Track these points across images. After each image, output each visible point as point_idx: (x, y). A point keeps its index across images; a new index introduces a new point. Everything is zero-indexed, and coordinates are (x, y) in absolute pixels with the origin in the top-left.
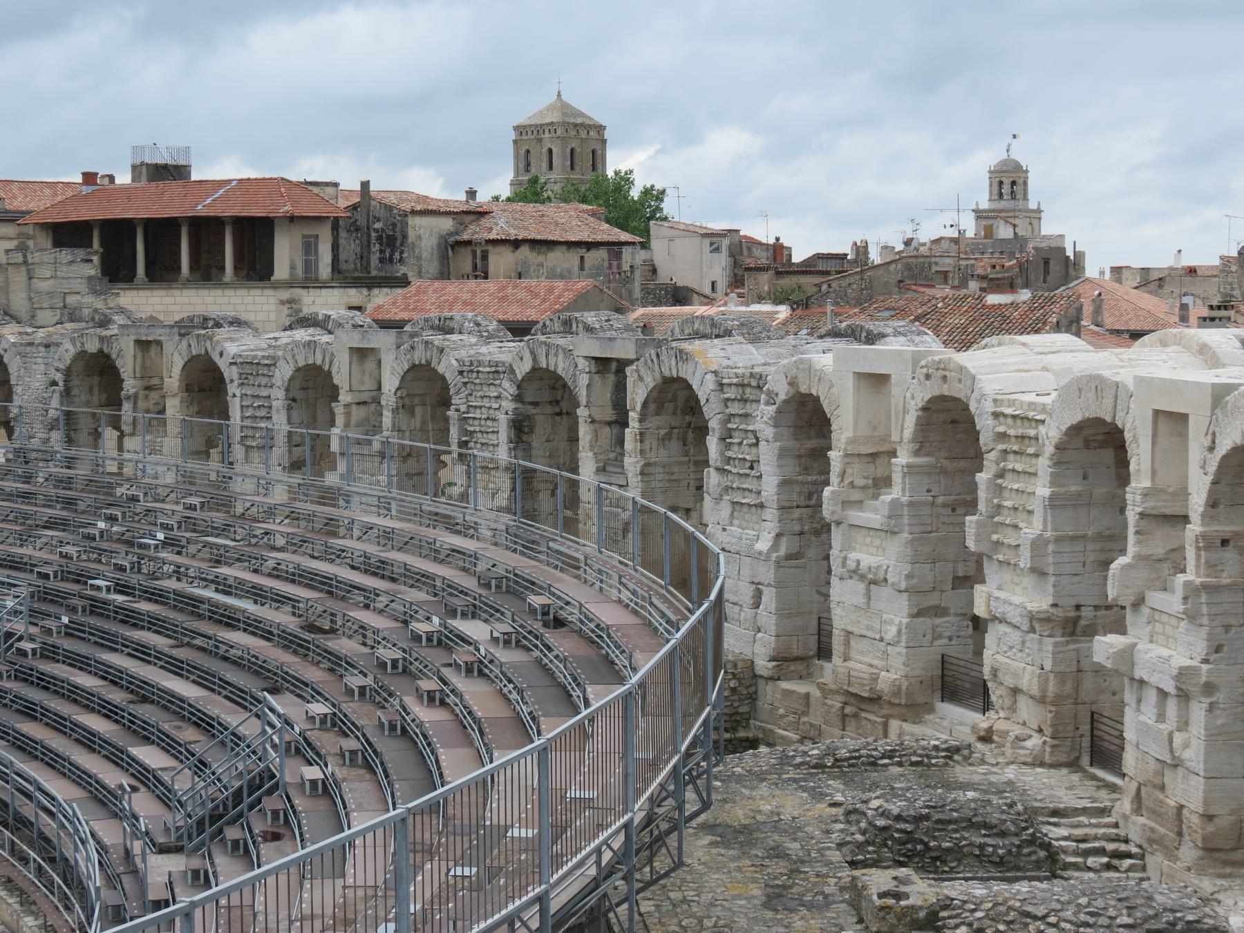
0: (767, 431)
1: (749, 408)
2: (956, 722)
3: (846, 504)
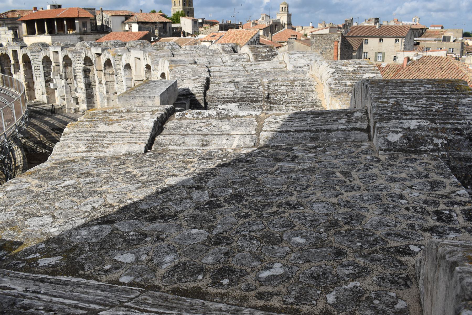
0: (123, 73)
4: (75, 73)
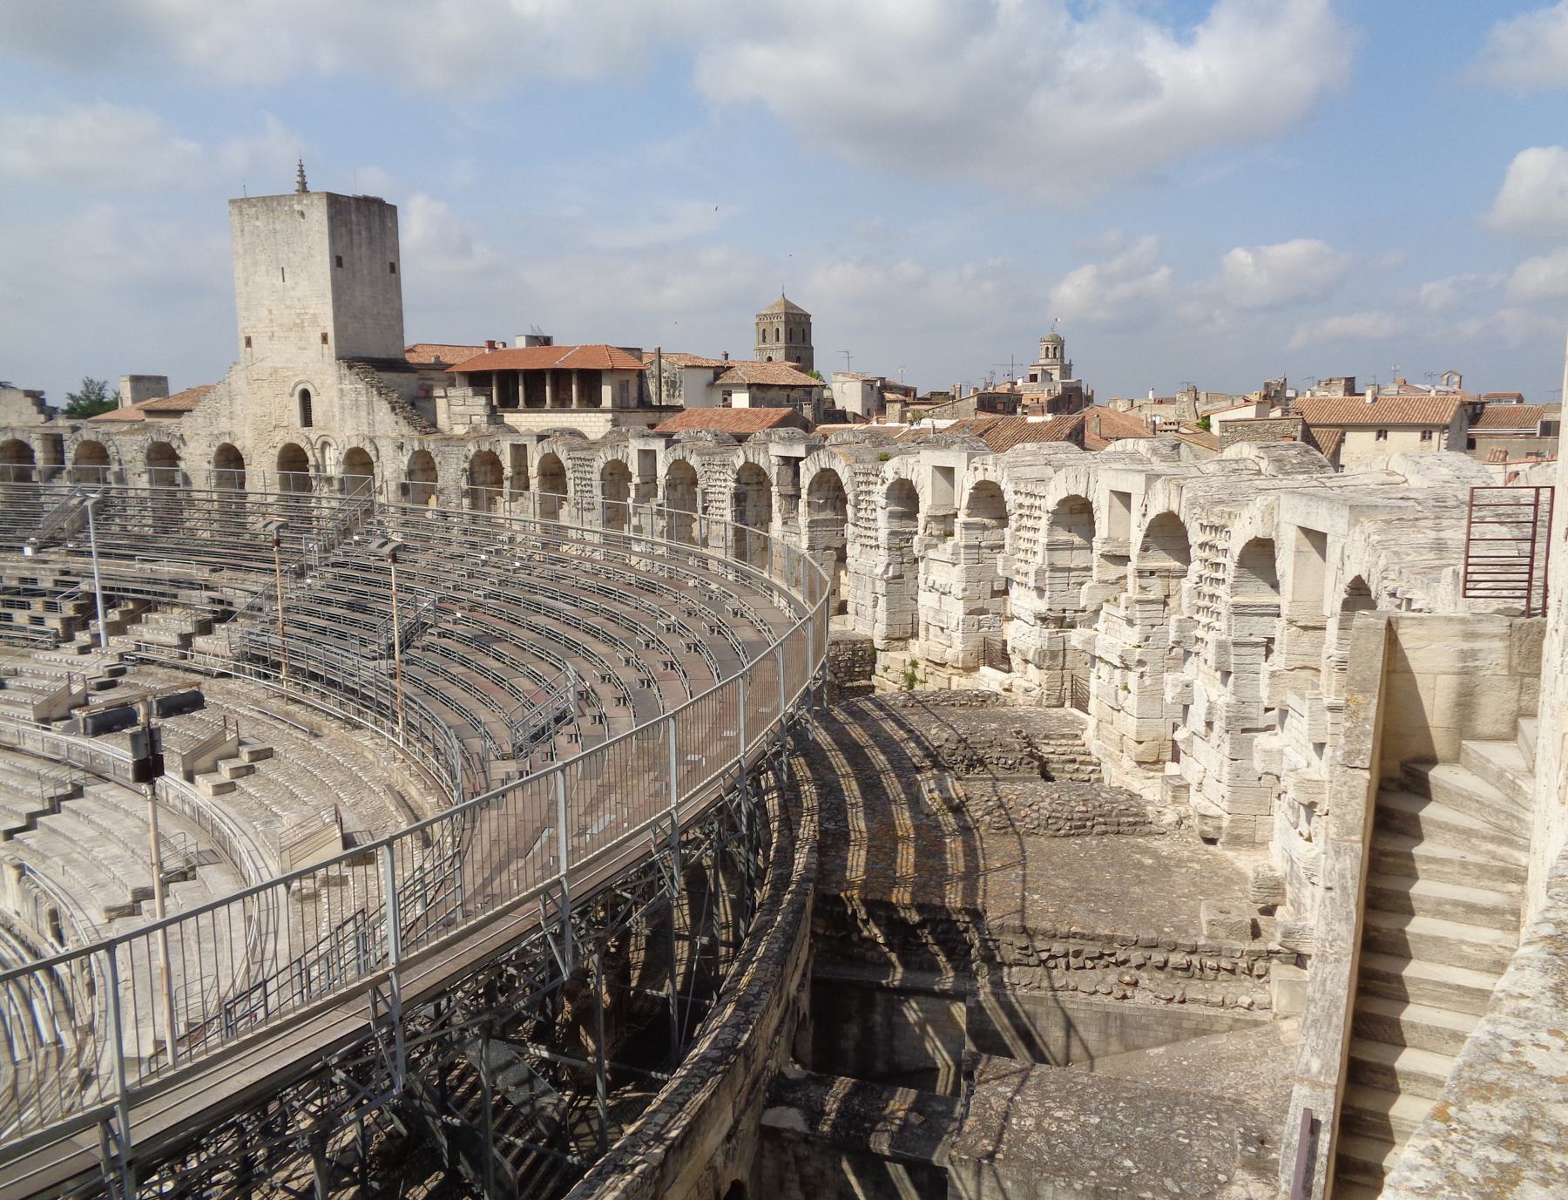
0: (883, 502)
1: (872, 487)
2: (989, 679)
3: (927, 547)
4: (704, 501)
